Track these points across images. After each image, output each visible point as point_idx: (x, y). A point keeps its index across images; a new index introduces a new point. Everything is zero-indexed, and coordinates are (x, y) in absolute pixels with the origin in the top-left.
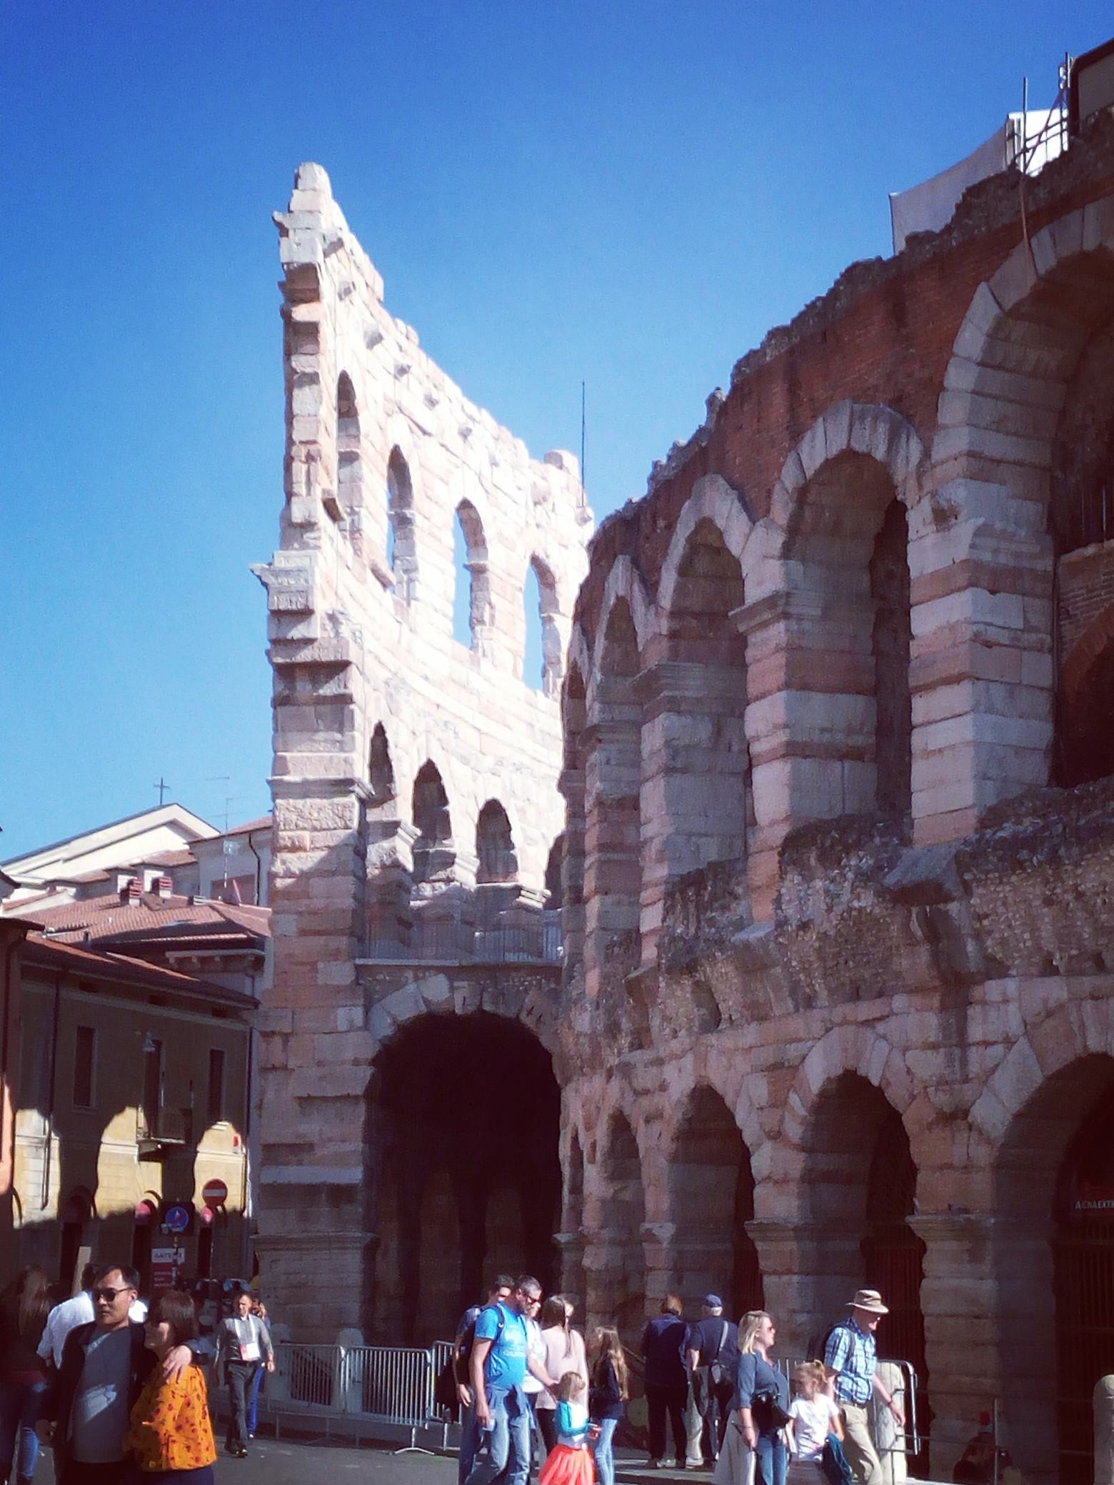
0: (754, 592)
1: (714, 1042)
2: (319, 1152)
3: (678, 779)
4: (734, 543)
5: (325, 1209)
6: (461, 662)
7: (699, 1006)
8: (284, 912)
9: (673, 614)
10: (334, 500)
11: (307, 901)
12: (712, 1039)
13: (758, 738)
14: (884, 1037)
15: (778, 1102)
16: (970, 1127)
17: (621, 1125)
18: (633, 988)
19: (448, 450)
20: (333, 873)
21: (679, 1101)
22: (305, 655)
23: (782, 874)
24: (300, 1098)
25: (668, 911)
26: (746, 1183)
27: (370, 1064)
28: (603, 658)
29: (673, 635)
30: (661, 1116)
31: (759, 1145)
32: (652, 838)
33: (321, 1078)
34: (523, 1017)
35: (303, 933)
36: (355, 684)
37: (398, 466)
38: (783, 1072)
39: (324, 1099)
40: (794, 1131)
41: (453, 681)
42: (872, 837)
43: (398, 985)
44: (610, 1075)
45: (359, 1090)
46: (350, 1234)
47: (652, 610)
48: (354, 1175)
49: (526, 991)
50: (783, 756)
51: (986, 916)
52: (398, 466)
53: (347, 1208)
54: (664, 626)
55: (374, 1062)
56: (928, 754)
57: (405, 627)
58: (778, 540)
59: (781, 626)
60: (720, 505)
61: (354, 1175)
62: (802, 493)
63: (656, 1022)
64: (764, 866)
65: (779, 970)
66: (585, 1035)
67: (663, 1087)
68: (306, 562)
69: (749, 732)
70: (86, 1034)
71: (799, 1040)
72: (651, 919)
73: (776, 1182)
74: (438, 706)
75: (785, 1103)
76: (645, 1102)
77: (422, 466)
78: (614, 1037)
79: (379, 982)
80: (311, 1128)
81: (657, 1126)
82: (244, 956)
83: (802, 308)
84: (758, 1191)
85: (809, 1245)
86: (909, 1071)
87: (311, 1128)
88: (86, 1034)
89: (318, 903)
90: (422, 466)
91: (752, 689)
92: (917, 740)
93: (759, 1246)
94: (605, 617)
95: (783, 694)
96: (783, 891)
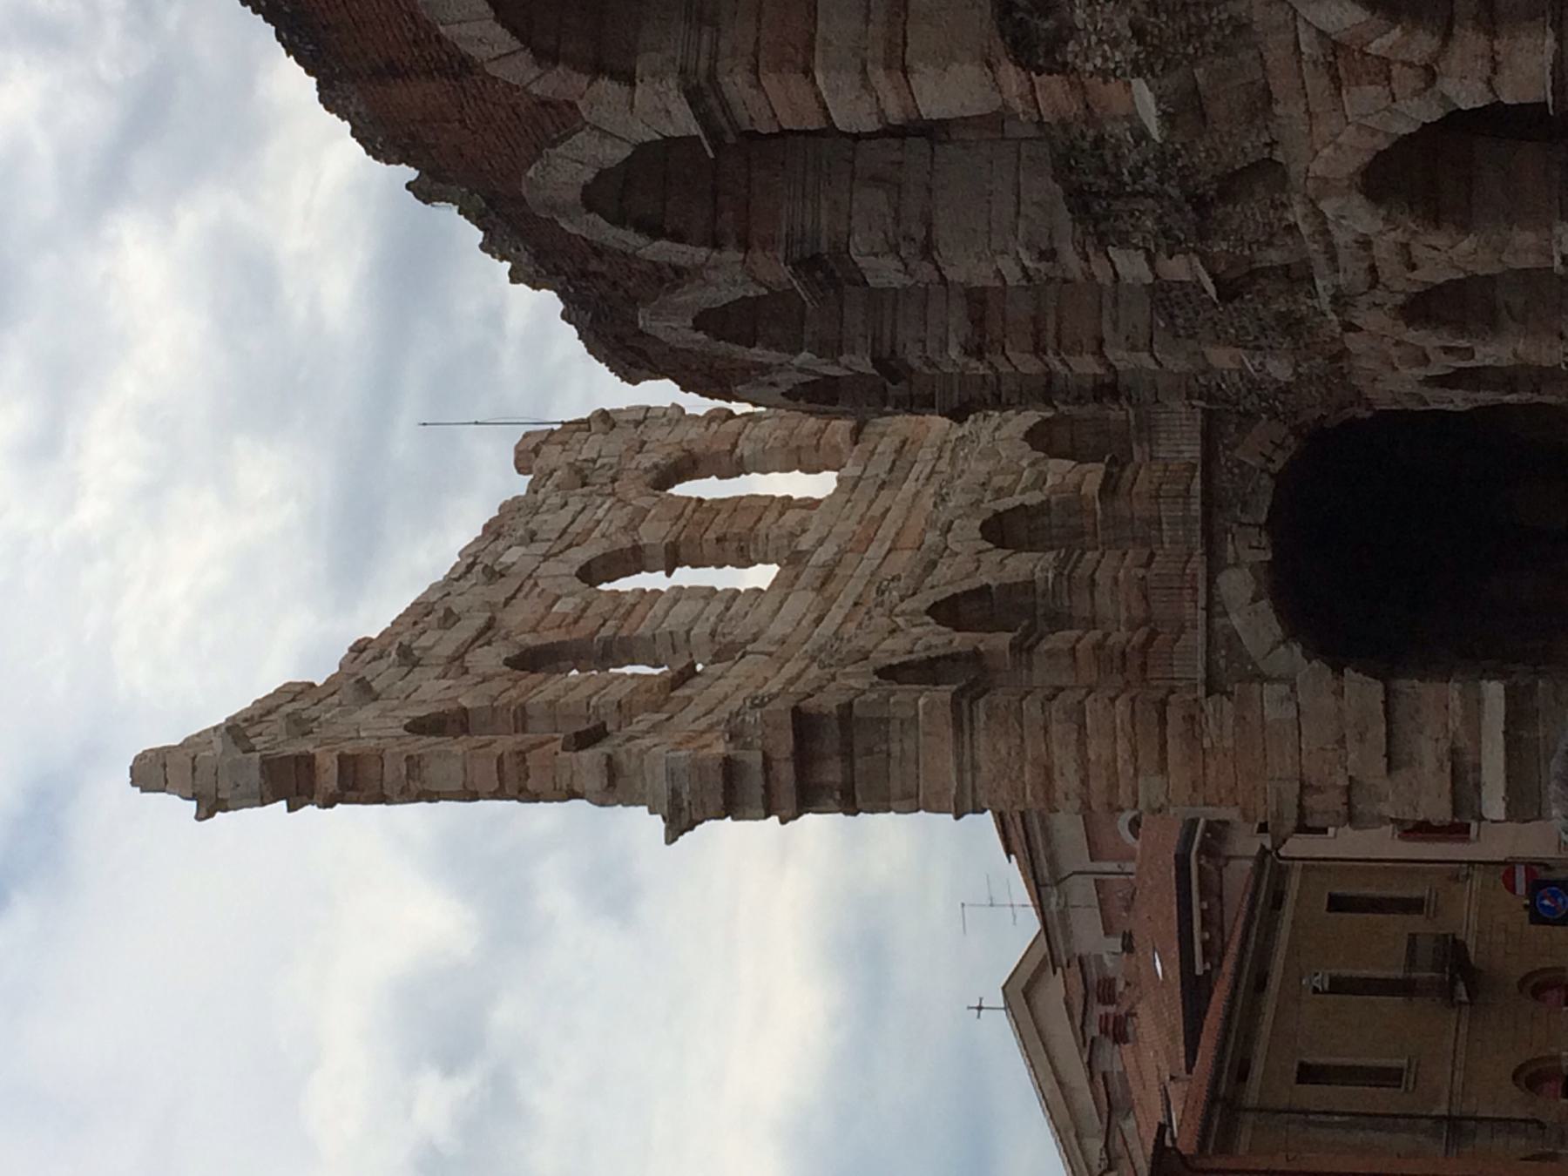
1: (1302, 167)
2: (1464, 742)
4: (616, 154)
6: (797, 577)
8: (1135, 793)
9: (717, 245)
10: (577, 734)
11: (1120, 764)
12: (1295, 170)
15: (1383, 69)
17: (1423, 307)
18: (1229, 291)
19: (513, 597)
20: (1082, 726)
21: (1386, 220)
22: (786, 772)
23: (1064, 69)
24: (1389, 769)
25: (1124, 242)
26: (1497, 120)
29: (745, 245)
30: (1405, 246)
32: (1024, 269)
33: (1361, 738)
34: (1275, 468)
35: (1163, 768)
36: (829, 702)
37: (531, 661)
38: (1340, 61)
39: (1389, 735)
40: (1424, 44)
41: (823, 584)
43: (1233, 638)
44: (1349, 327)
48: (1494, 691)
49: (1241, 464)
50: (905, 71)
52: (531, 661)
55: (1338, 671)
57: (749, 648)
58: (607, 87)
59: (725, 80)
60: (562, 173)
62: (545, 56)
63: (1274, 256)
64: (1054, 93)
67: (1365, 243)
68: (661, 770)
69: (870, 124)
70: (1308, 1074)
71: (1297, 45)
72: (1132, 266)
73: (1494, 71)
74: (856, 604)
75: (1385, 62)
77: (534, 630)
78: (1300, 321)
80: (1428, 752)
81: (1419, 252)
82: (1200, 867)
84: (1507, 99)
87: (1428, 752)
88: (1308, 1074)
89: (1122, 748)
90: (534, 630)
91: (815, 123)
96: (1089, 67)
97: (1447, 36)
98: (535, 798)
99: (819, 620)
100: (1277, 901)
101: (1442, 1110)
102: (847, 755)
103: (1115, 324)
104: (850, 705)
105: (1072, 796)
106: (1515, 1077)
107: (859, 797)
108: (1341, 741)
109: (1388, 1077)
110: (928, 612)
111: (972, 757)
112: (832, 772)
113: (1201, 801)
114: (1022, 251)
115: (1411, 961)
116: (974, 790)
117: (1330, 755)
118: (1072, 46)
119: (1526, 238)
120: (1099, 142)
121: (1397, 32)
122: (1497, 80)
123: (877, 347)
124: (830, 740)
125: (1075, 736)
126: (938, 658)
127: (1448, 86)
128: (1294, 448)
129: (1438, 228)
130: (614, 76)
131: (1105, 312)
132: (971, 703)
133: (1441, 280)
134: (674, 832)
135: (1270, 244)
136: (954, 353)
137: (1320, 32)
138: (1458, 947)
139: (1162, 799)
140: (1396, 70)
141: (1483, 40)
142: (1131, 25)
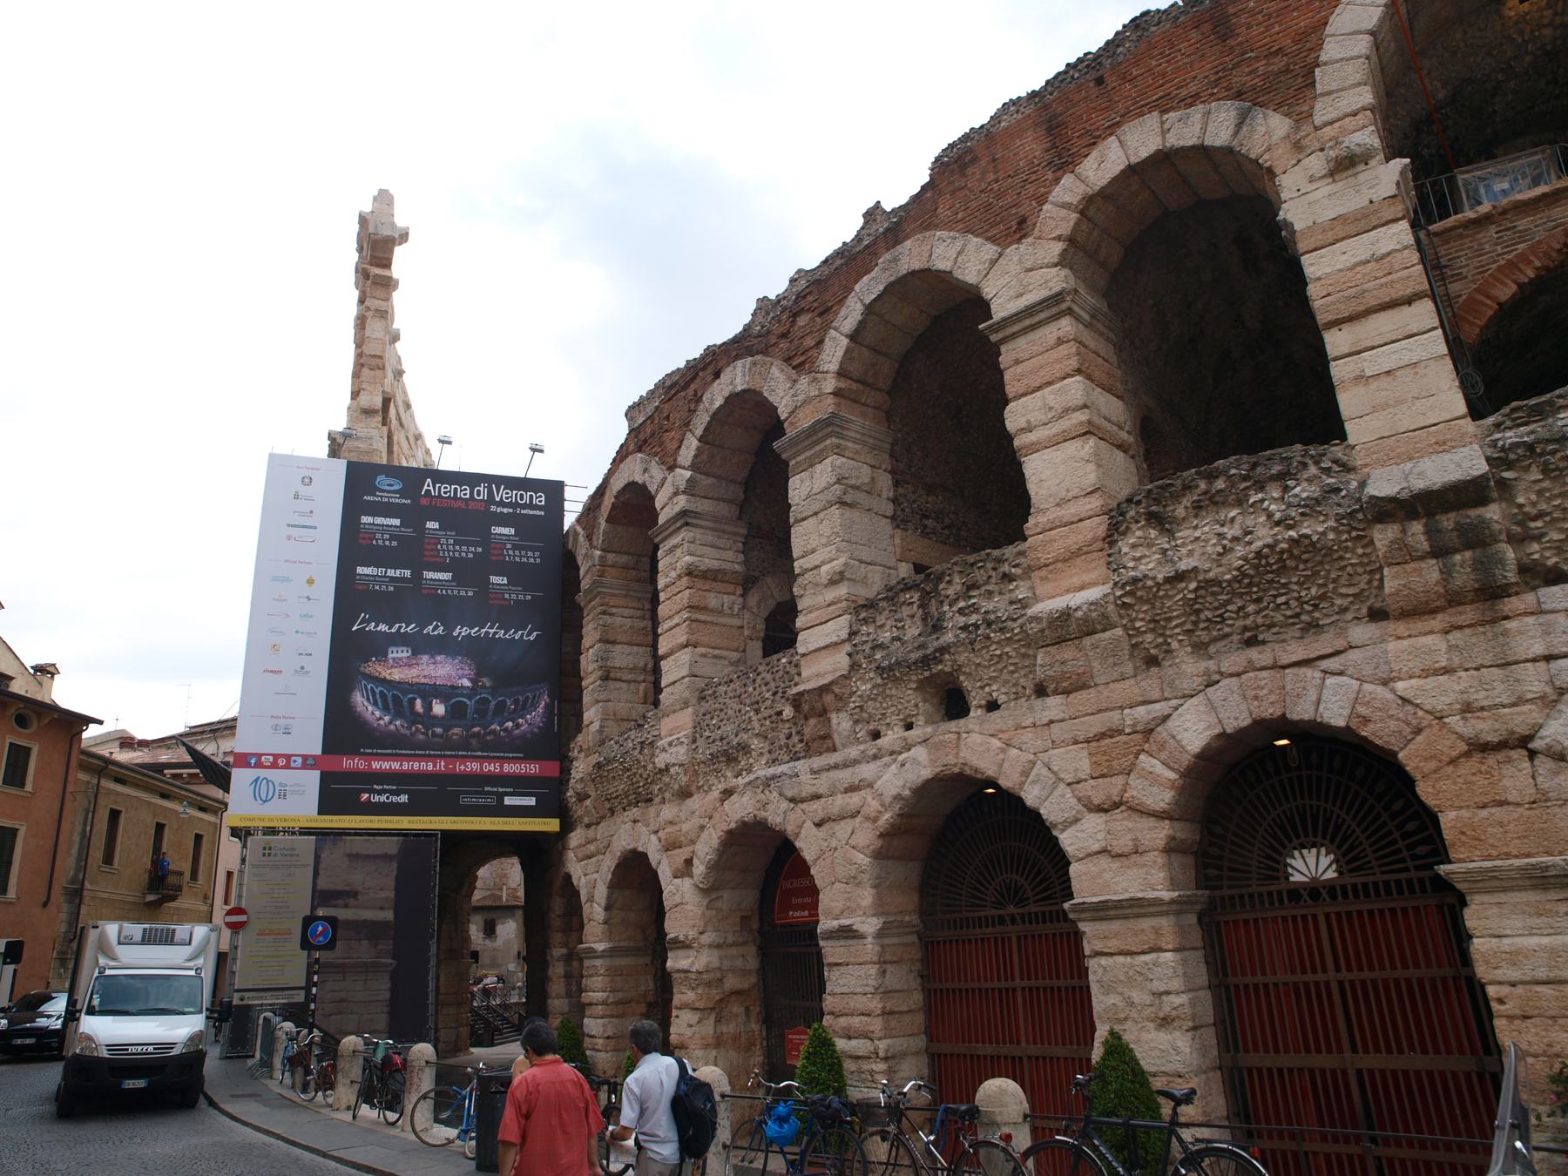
0: (1001, 308)
3: (848, 512)
7: (925, 701)
9: (841, 373)
13: (1029, 429)
14: (1341, 674)
16: (1532, 754)
28: (696, 456)
31: (1076, 820)
40: (1162, 798)
42: (1305, 466)
44: (728, 793)
47: (804, 380)
51: (1535, 519)
54: (830, 385)
56: (1362, 379)
65: (1119, 632)
70: (115, 815)
76: (815, 806)
83: (1062, 68)
84: (1074, 869)
85: (1172, 919)
86: (1405, 700)
88: (115, 815)
92: (1338, 371)
93: (1083, 926)
94: (701, 422)
95: (1078, 378)
97: (1159, 815)
98: (356, 375)
100: (203, 809)
101: (88, 885)
103: (704, 655)
109: (108, 858)
114: (842, 560)
118: (1153, 533)
119: (866, 897)
120: (1008, 578)
121: (1172, 775)
122: (1104, 861)
127: (1093, 822)
129: (881, 835)
130: (1064, 253)
135: (856, 722)
137: (1166, 718)
138: (174, 898)
140: (1120, 780)
141: (1161, 843)
142: (1195, 569)
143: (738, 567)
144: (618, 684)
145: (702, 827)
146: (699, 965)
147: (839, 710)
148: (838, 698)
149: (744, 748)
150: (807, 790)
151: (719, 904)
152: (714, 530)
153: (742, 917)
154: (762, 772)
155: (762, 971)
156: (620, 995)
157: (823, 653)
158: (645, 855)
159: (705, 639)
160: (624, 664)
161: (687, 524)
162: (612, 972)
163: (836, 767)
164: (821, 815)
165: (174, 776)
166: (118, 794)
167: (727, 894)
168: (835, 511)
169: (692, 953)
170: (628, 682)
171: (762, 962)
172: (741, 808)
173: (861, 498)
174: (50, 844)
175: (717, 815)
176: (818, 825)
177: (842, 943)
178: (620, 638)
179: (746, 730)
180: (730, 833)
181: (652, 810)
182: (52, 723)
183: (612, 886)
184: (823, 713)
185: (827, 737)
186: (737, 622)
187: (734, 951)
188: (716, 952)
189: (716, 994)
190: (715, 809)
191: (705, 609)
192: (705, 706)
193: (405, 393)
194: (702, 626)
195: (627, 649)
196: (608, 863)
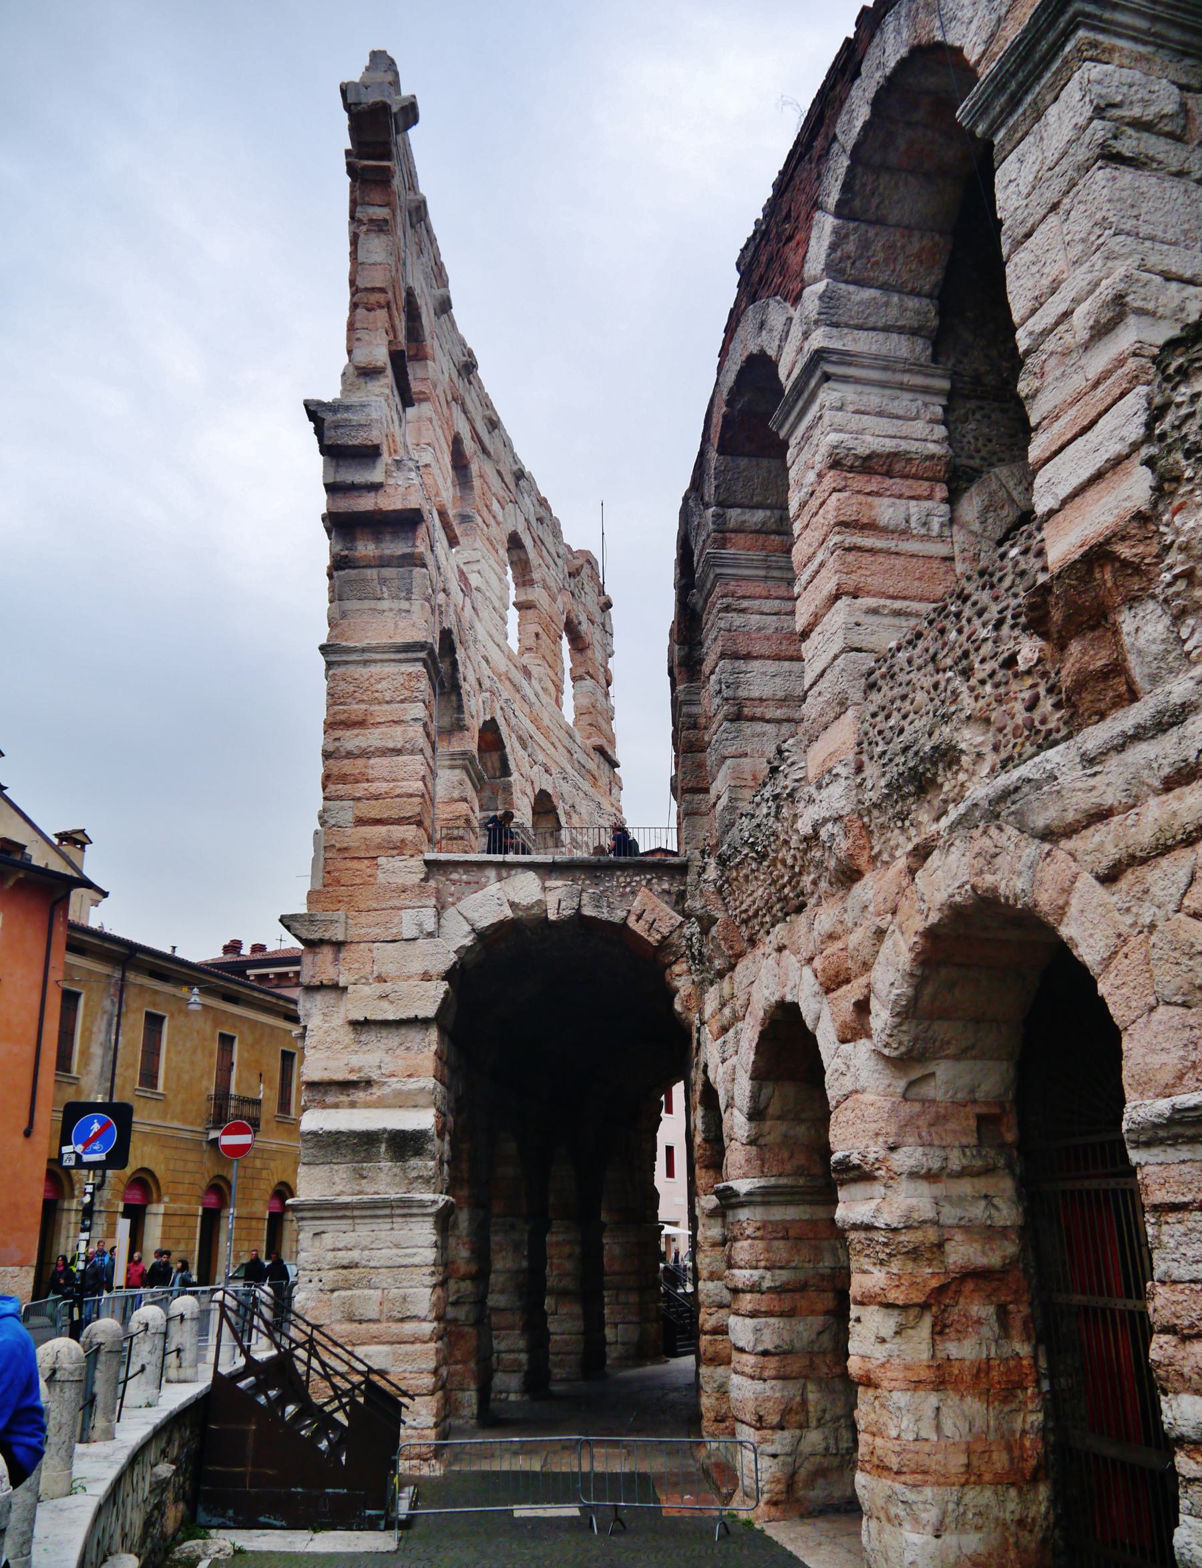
2: (376, 1092)
3: (1127, 176)
5: (385, 1164)
8: (340, 798)
11: (366, 785)
20: (398, 752)
22: (366, 503)
27: (443, 979)
28: (833, 247)
34: (632, 923)
43: (479, 886)
44: (922, 853)
45: (430, 1010)
46: (417, 1196)
48: (424, 1119)
49: (633, 893)
53: (414, 1162)
55: (448, 976)
61: (424, 1119)
66: (838, 819)
79: (454, 882)
99: (487, 661)
102: (383, 562)
103: (875, 611)
104: (424, 566)
105: (337, 744)
106: (143, 1170)
107: (342, 573)
108: (381, 979)
110: (493, 720)
111: (375, 661)
112: (366, 548)
113: (330, 855)
115: (243, 1101)
116: (347, 663)
117: (368, 969)
123: (834, 358)
124: (396, 548)
125: (391, 746)
126: (460, 695)
128: (650, 939)
131: (888, 602)
132: (423, 660)
133: (1066, 931)
134: (315, 412)
136: (833, 438)
139: (332, 822)
143: (933, 448)
144: (759, 727)
145: (880, 933)
146: (889, 1216)
147: (1132, 601)
148: (1133, 568)
149: (947, 756)
150: (1079, 802)
151: (931, 1090)
152: (883, 385)
153: (981, 1119)
154: (980, 790)
155: (1029, 1233)
156: (783, 1276)
157: (1092, 494)
158: (795, 1007)
159: (875, 582)
160: (767, 692)
161: (827, 377)
162: (770, 1232)
163: (1139, 735)
164: (1112, 853)
165: (262, 978)
166: (156, 992)
167: (943, 1070)
168: (1100, 175)
169: (878, 1189)
170: (779, 721)
171: (1028, 1213)
172: (947, 879)
173: (1155, 146)
174: (29, 1050)
175: (904, 905)
176: (1109, 877)
177: (1185, 1153)
178: (757, 649)
179: (946, 718)
180: (930, 934)
181: (803, 919)
182: (19, 884)
183: (759, 1075)
184: (1095, 619)
185: (1117, 669)
186: (942, 549)
187: (965, 1187)
188: (924, 1187)
189: (928, 1275)
190: (901, 892)
191: (870, 527)
192: (877, 698)
193: (487, 404)
194: (867, 559)
195: (772, 667)
196: (749, 1032)
